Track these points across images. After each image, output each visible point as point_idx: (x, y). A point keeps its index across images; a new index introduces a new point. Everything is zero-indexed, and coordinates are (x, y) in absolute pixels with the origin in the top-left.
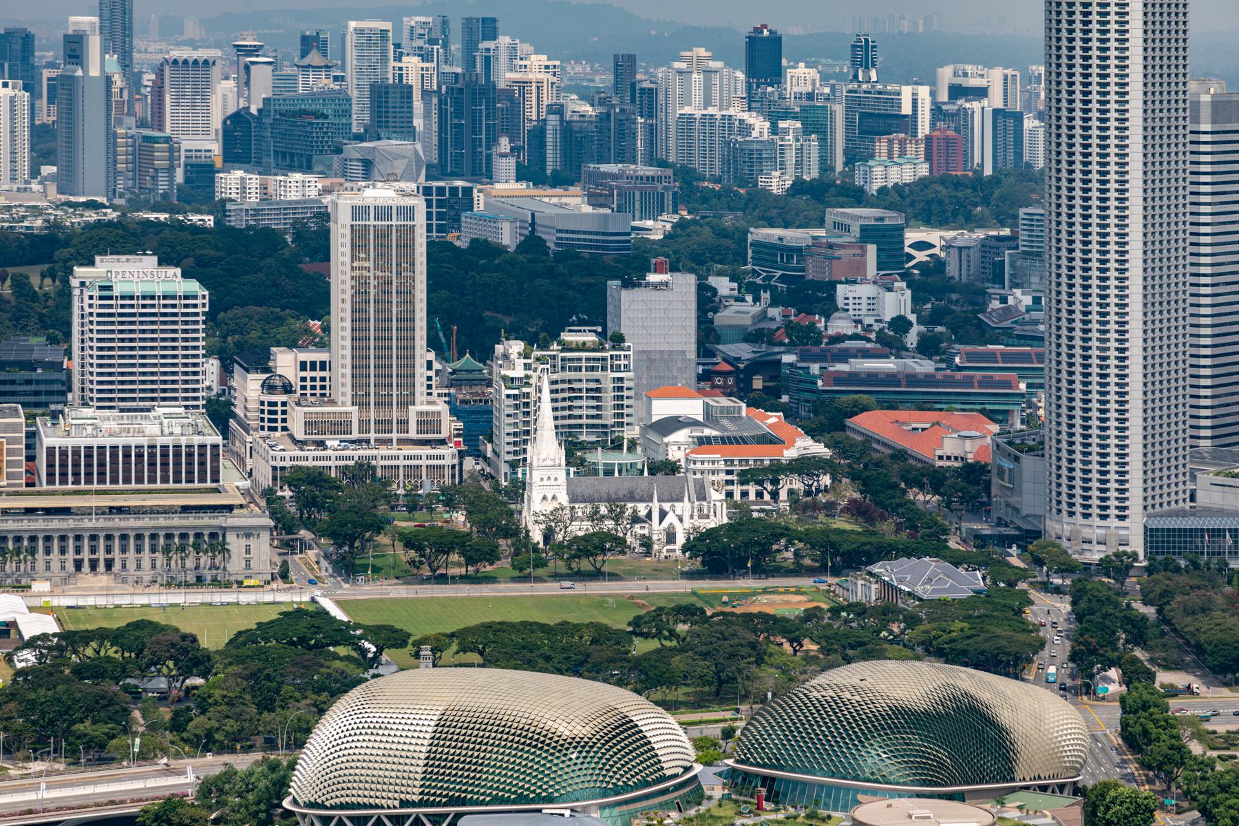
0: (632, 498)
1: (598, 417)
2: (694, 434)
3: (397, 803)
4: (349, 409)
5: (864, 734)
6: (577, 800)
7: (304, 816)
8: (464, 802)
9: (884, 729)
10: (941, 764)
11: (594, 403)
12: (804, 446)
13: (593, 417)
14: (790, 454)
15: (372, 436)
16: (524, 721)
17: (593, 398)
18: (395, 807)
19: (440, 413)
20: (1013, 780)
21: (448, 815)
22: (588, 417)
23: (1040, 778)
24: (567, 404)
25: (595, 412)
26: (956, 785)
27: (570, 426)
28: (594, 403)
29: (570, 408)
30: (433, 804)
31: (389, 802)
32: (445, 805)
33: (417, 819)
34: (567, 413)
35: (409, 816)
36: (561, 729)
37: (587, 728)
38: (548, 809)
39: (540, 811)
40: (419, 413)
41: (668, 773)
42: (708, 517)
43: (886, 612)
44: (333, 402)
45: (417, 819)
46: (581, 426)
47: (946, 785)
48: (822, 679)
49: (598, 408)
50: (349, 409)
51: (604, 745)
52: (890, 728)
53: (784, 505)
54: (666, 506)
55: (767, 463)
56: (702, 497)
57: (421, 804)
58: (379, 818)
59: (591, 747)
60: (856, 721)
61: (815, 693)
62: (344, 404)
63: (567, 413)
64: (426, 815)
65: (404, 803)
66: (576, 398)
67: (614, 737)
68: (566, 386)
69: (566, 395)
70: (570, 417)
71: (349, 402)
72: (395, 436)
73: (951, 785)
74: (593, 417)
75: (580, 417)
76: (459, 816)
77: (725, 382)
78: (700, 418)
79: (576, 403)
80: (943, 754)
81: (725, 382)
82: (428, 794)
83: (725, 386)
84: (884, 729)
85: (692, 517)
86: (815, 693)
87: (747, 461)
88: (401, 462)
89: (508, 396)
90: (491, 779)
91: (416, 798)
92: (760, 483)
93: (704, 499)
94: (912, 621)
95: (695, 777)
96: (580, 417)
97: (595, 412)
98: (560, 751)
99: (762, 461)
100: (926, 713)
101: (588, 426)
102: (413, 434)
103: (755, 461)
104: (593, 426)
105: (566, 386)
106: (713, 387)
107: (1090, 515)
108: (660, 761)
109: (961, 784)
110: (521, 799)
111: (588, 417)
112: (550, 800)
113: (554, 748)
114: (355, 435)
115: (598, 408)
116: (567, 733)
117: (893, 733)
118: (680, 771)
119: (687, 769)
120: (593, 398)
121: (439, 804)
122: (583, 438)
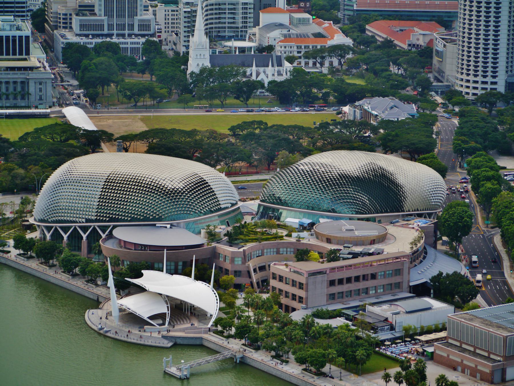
0: (243, 65)
1: (233, 23)
2: (282, 33)
3: (84, 220)
4: (103, 18)
5: (325, 188)
6: (174, 220)
7: (39, 226)
8: (118, 220)
9: (335, 185)
10: (364, 204)
11: (232, 16)
12: (339, 39)
13: (231, 23)
14: (330, 43)
15: (115, 32)
16: (148, 180)
17: (231, 13)
18: (83, 222)
19: (149, 21)
20: (403, 211)
21: (109, 226)
22: (228, 23)
23: (418, 210)
24: (218, 16)
25: (232, 21)
26: (371, 213)
27: (219, 28)
28: (232, 16)
29: (219, 18)
30: (102, 221)
31: (80, 220)
32: (108, 221)
33: (94, 228)
34: (218, 21)
35: (90, 227)
36: (167, 184)
37: (181, 184)
38: (158, 224)
39: (155, 225)
40: (140, 21)
41: (222, 206)
42: (282, 75)
43: (364, 124)
44: (95, 14)
45: (94, 228)
46: (225, 28)
47: (366, 214)
48: (307, 160)
49: (234, 18)
50: (103, 18)
51: (189, 192)
52: (338, 185)
53: (325, 70)
54: (261, 69)
55: (319, 47)
56: (280, 64)
57: (96, 221)
58: (75, 228)
59: (182, 193)
60: (321, 181)
61: (302, 167)
62: (100, 16)
63: (218, 21)
64: (99, 226)
65: (88, 221)
66: (222, 13)
67: (195, 188)
68: (217, 7)
69: (218, 11)
70: (219, 23)
71: (103, 15)
72: (127, 32)
73: (369, 214)
74: (231, 23)
75: (225, 23)
76: (114, 227)
77: (305, 5)
78: (288, 24)
79: (222, 16)
80: (365, 199)
81: (305, 5)
82: (100, 216)
83: (305, 7)
84: (335, 185)
85: (273, 75)
86: (302, 167)
87: (309, 47)
88: (129, 46)
89: (185, 12)
90: (133, 208)
91: (94, 218)
92: (315, 58)
93: (281, 66)
94: (374, 130)
95: (239, 208)
96: (225, 23)
97: (232, 21)
98: (166, 195)
99: (316, 47)
100: (358, 178)
101: (229, 27)
102: (136, 31)
103: (313, 47)
104: (231, 28)
105: (217, 7)
106: (300, 7)
107: (478, 75)
108: (218, 201)
109: (374, 213)
110: (146, 219)
111: (228, 23)
112: (160, 219)
113: (163, 194)
114: (106, 31)
115: (234, 18)
116: (170, 186)
117: (339, 188)
118: (230, 205)
119: (233, 205)
120: (231, 13)
121: (105, 221)
122: (227, 34)
